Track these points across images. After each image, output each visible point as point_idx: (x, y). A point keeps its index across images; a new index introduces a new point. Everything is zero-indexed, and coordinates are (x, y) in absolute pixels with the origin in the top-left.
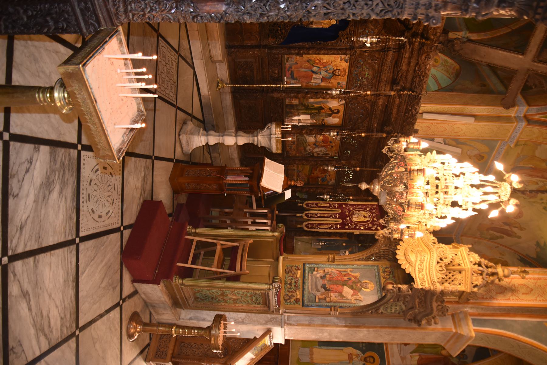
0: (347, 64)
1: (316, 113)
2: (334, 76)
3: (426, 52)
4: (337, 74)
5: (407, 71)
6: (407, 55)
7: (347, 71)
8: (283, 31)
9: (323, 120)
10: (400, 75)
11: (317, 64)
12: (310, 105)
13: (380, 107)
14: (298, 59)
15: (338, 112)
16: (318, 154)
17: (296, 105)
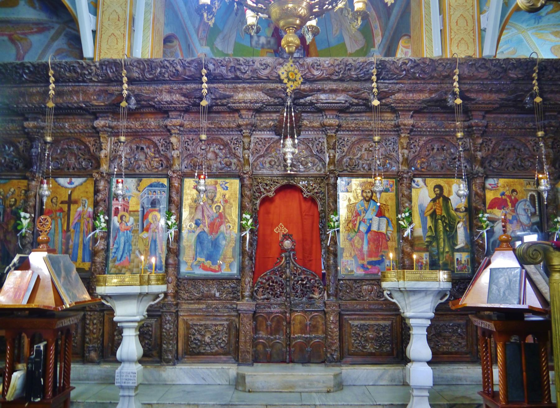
0: (355, 182)
1: (443, 222)
2: (373, 198)
3: (310, 71)
4: (369, 195)
5: (344, 91)
6: (323, 97)
8: (303, 276)
9: (457, 210)
10: (356, 101)
11: (355, 225)
12: (429, 234)
13: (423, 122)
14: (348, 255)
15: (440, 187)
16: (533, 214)
17: (431, 256)
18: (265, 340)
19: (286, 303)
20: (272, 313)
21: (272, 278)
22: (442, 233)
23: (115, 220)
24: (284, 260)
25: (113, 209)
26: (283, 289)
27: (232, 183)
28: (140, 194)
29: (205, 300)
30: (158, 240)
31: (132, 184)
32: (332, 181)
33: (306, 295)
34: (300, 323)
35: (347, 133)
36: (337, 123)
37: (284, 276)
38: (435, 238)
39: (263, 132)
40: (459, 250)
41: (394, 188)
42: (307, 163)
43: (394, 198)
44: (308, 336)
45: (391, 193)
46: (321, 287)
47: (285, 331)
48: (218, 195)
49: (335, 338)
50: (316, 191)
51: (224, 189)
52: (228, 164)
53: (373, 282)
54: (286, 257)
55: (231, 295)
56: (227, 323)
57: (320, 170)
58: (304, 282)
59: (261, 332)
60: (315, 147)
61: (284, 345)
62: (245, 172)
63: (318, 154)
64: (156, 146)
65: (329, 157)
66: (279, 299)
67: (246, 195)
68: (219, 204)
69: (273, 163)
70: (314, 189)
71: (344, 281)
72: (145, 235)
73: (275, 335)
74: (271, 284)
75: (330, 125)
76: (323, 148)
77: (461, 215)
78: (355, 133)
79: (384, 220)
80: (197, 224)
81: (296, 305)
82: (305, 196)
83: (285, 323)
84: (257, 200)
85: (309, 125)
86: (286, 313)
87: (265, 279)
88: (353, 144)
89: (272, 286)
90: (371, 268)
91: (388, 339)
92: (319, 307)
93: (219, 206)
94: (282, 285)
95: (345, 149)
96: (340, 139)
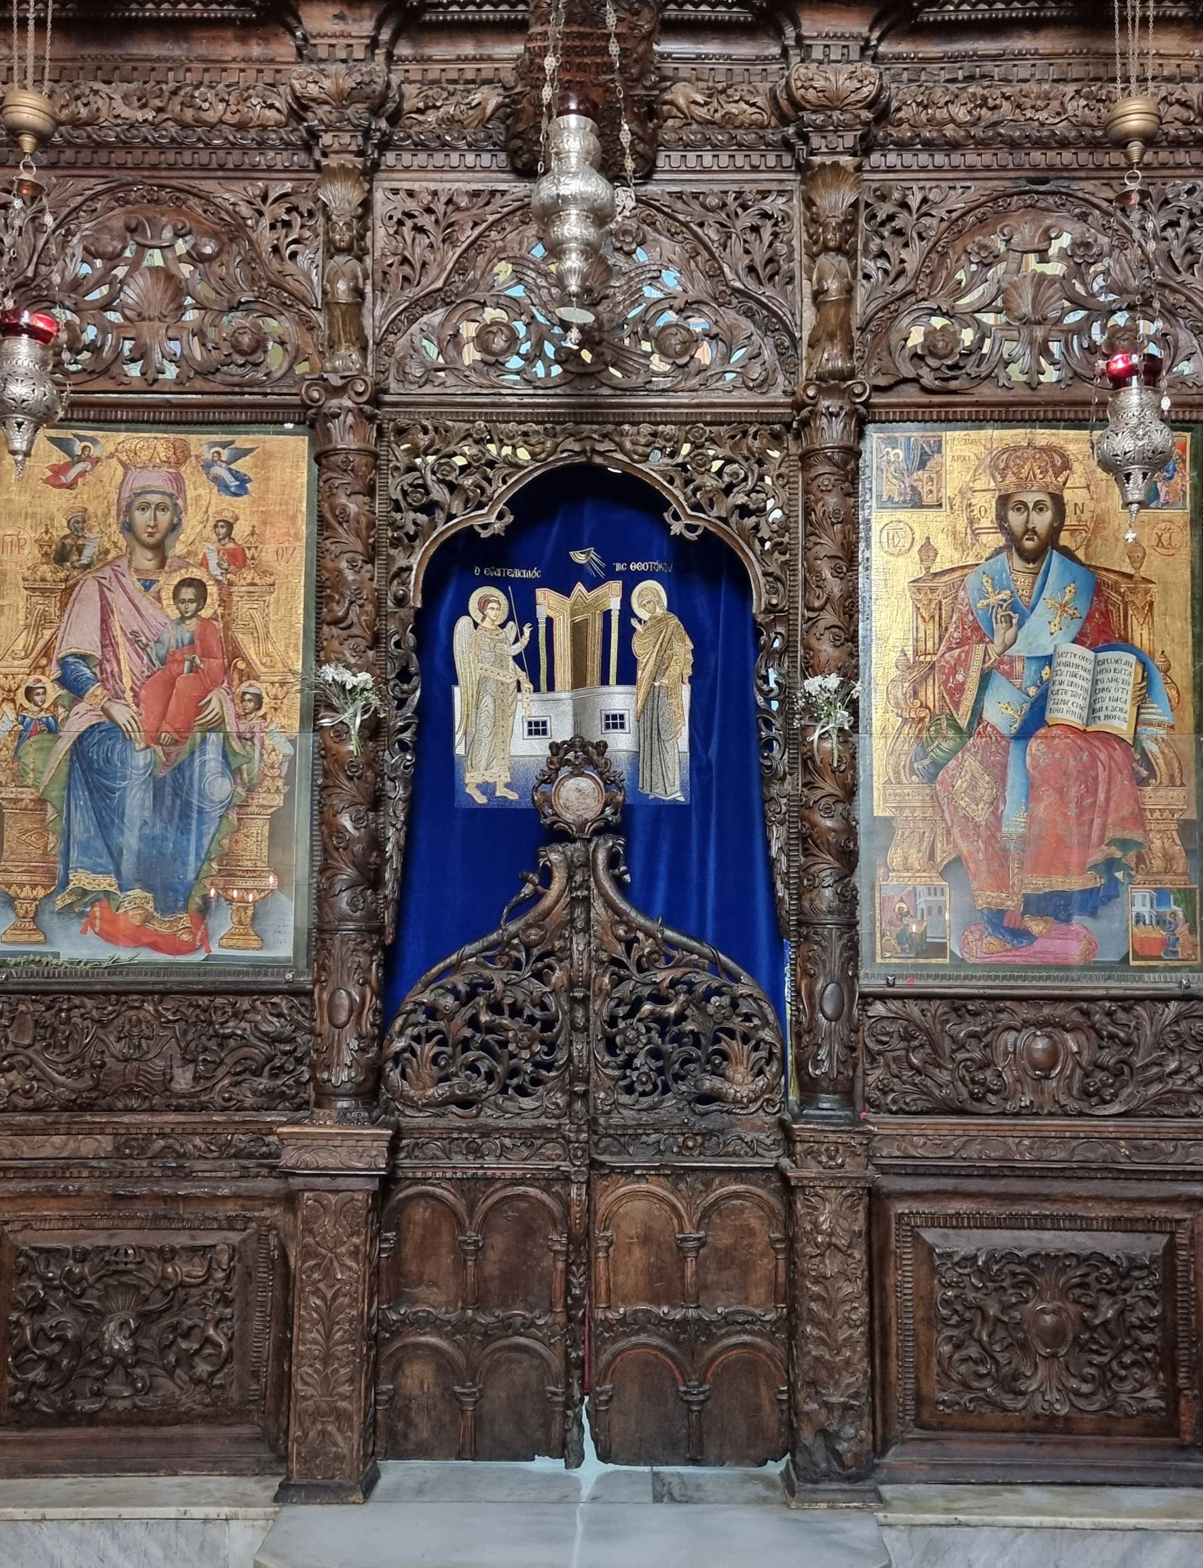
2: (1065, 539)
4: (1042, 521)
7: (1016, 436)
8: (663, 976)
14: (915, 858)
18: (449, 1336)
19: (568, 1128)
20: (491, 1180)
21: (489, 985)
24: (556, 886)
26: (552, 1047)
27: (269, 456)
29: (110, 1110)
32: (832, 433)
33: (677, 1077)
34: (646, 1238)
35: (924, 159)
36: (868, 90)
37: (557, 976)
39: (439, 159)
42: (691, 342)
44: (692, 1313)
45: (1166, 513)
46: (767, 1035)
47: (558, 1286)
48: (192, 525)
49: (842, 1335)
50: (741, 499)
51: (224, 487)
52: (246, 340)
53: (1060, 1010)
54: (571, 868)
55: (263, 1083)
56: (235, 1237)
57: (765, 383)
58: (672, 1010)
59: (421, 1291)
60: (736, 246)
61: (557, 1364)
62: (335, 381)
63: (752, 286)
65: (818, 295)
66: (526, 1103)
67: (343, 517)
68: (197, 573)
69: (499, 343)
70: (728, 490)
71: (895, 1005)
73: (505, 1305)
74: (484, 1018)
75: (831, 102)
76: (782, 249)
78: (972, 159)
80: (73, 686)
81: (625, 1138)
82: (677, 528)
83: (558, 1240)
84: (410, 551)
85: (702, 112)
86: (567, 1179)
87: (454, 991)
88: (956, 226)
89: (490, 1029)
90: (1047, 936)
91: (1147, 1338)
92: (753, 1148)
93: (199, 586)
94: (548, 1025)
95: (912, 257)
96: (883, 198)
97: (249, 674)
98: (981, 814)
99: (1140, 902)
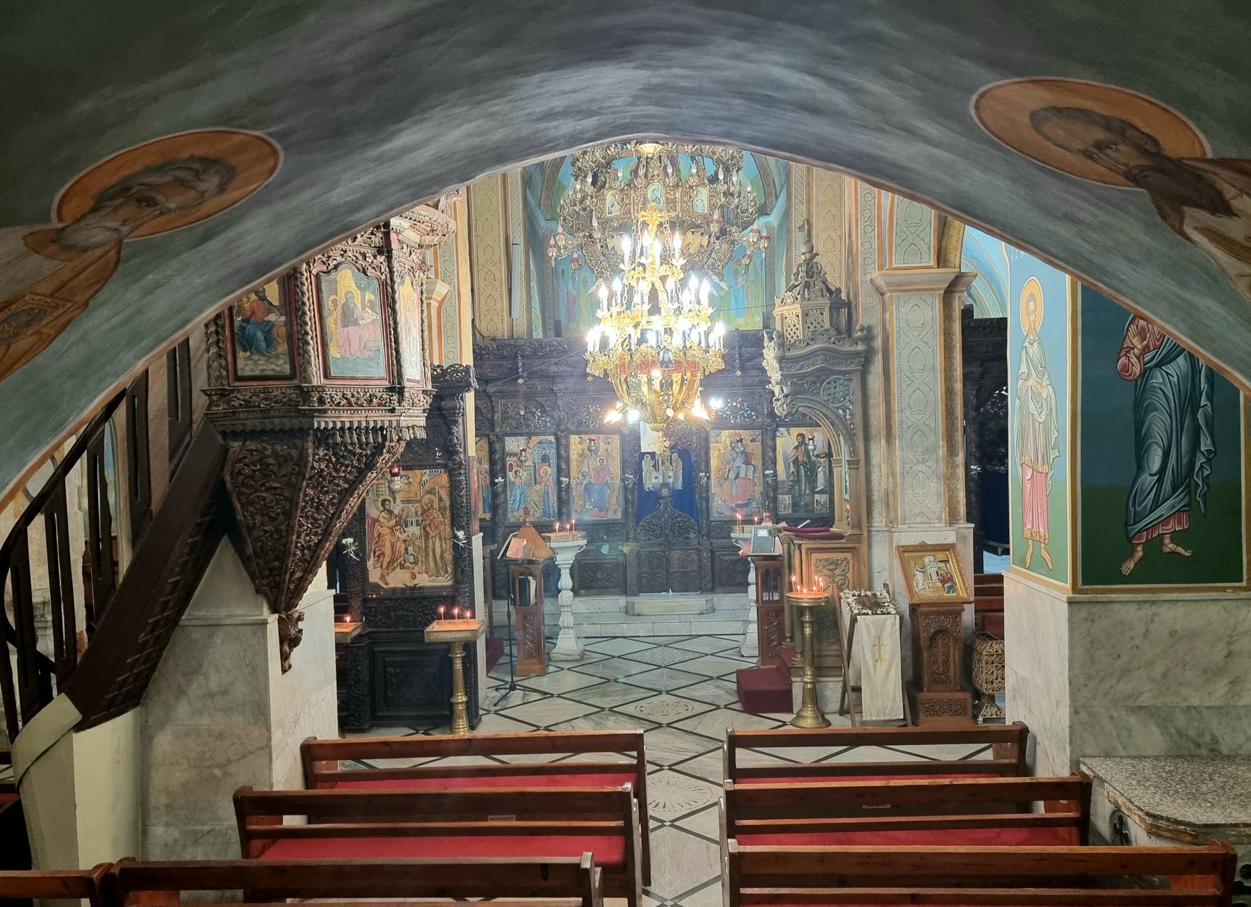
8: (679, 519)
9: (817, 456)
12: (791, 478)
22: (803, 477)
23: (511, 475)
25: (508, 465)
28: (531, 450)
30: (550, 491)
31: (523, 442)
34: (678, 559)
38: (798, 482)
40: (818, 492)
41: (760, 437)
43: (760, 447)
48: (601, 450)
64: (542, 406)
72: (538, 487)
77: (822, 460)
79: (751, 468)
92: (694, 545)
97: (612, 474)
98: (729, 492)
99: (754, 504)
